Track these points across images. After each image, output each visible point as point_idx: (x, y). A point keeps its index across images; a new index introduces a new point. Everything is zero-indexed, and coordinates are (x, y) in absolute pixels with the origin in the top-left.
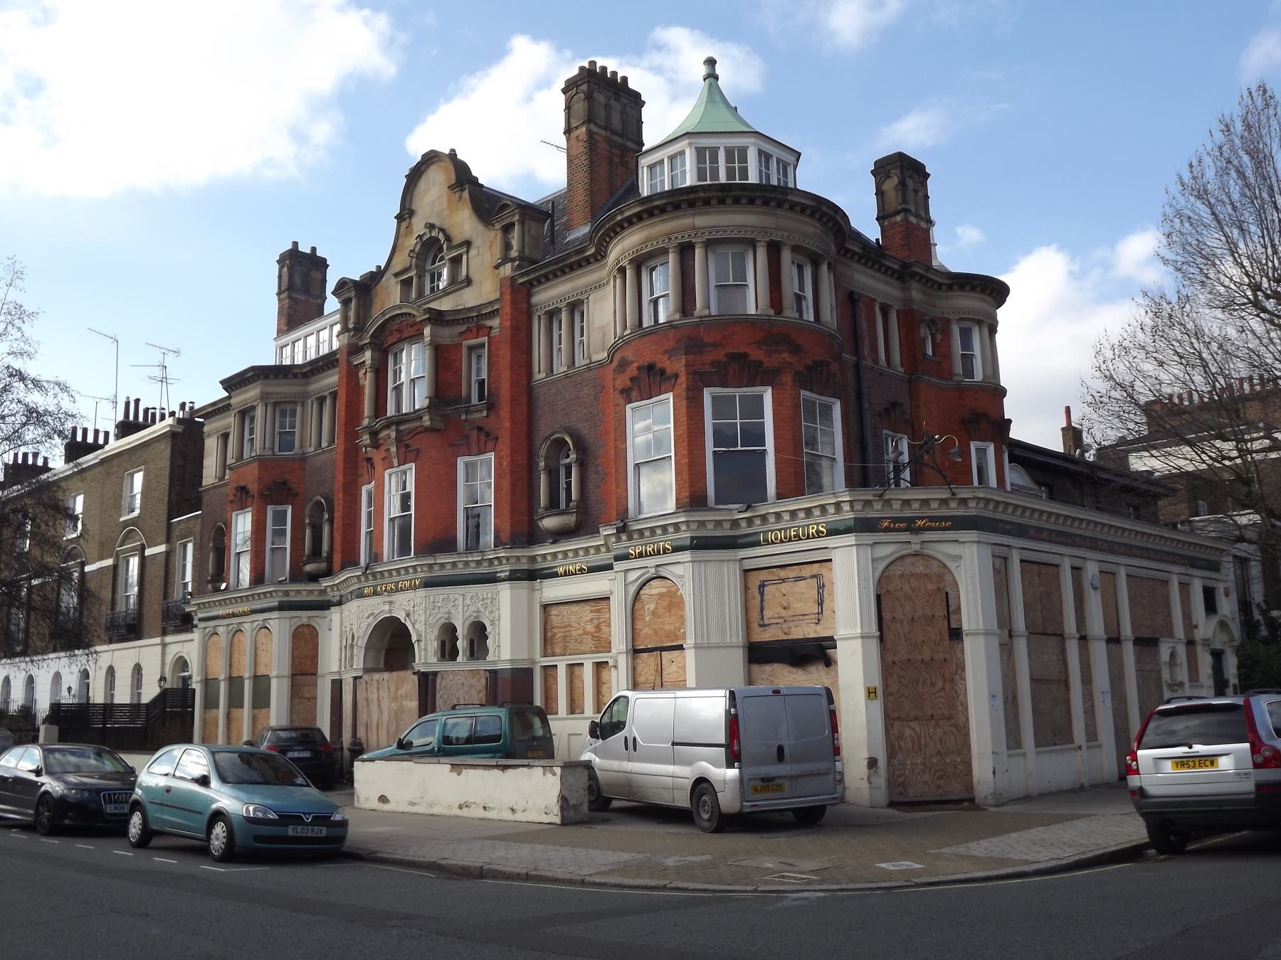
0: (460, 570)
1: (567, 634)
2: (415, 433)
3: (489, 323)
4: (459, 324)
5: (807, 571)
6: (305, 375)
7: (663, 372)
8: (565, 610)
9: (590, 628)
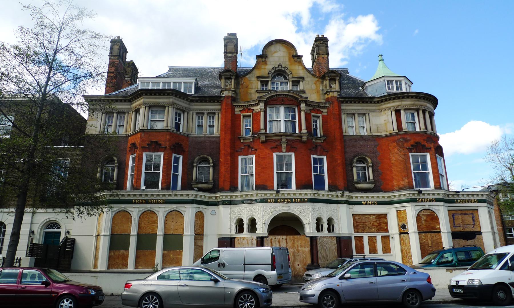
0: (326, 198)
1: (364, 225)
2: (294, 141)
3: (321, 110)
4: (310, 106)
5: (470, 212)
6: (192, 101)
7: (424, 146)
8: (363, 217)
9: (376, 224)
